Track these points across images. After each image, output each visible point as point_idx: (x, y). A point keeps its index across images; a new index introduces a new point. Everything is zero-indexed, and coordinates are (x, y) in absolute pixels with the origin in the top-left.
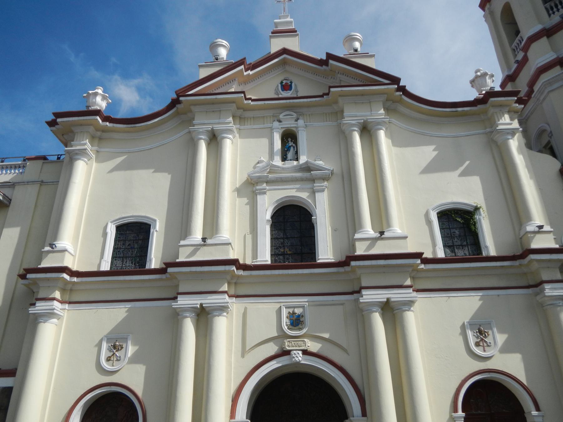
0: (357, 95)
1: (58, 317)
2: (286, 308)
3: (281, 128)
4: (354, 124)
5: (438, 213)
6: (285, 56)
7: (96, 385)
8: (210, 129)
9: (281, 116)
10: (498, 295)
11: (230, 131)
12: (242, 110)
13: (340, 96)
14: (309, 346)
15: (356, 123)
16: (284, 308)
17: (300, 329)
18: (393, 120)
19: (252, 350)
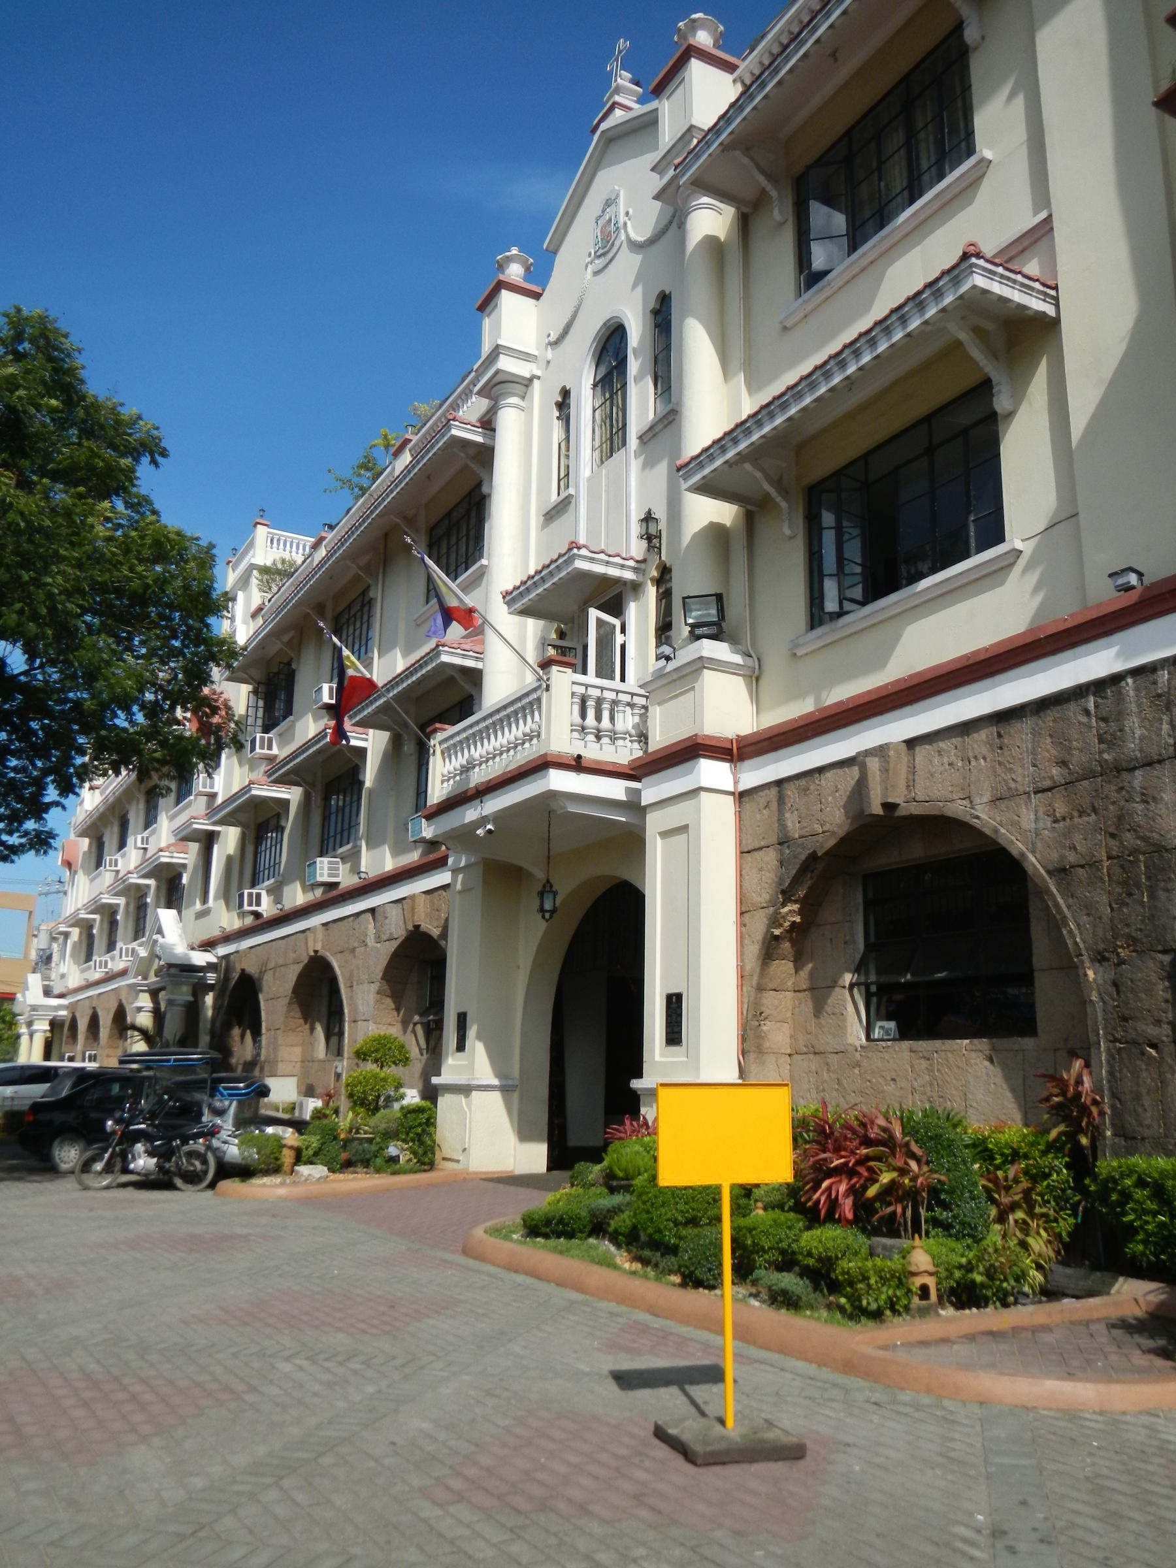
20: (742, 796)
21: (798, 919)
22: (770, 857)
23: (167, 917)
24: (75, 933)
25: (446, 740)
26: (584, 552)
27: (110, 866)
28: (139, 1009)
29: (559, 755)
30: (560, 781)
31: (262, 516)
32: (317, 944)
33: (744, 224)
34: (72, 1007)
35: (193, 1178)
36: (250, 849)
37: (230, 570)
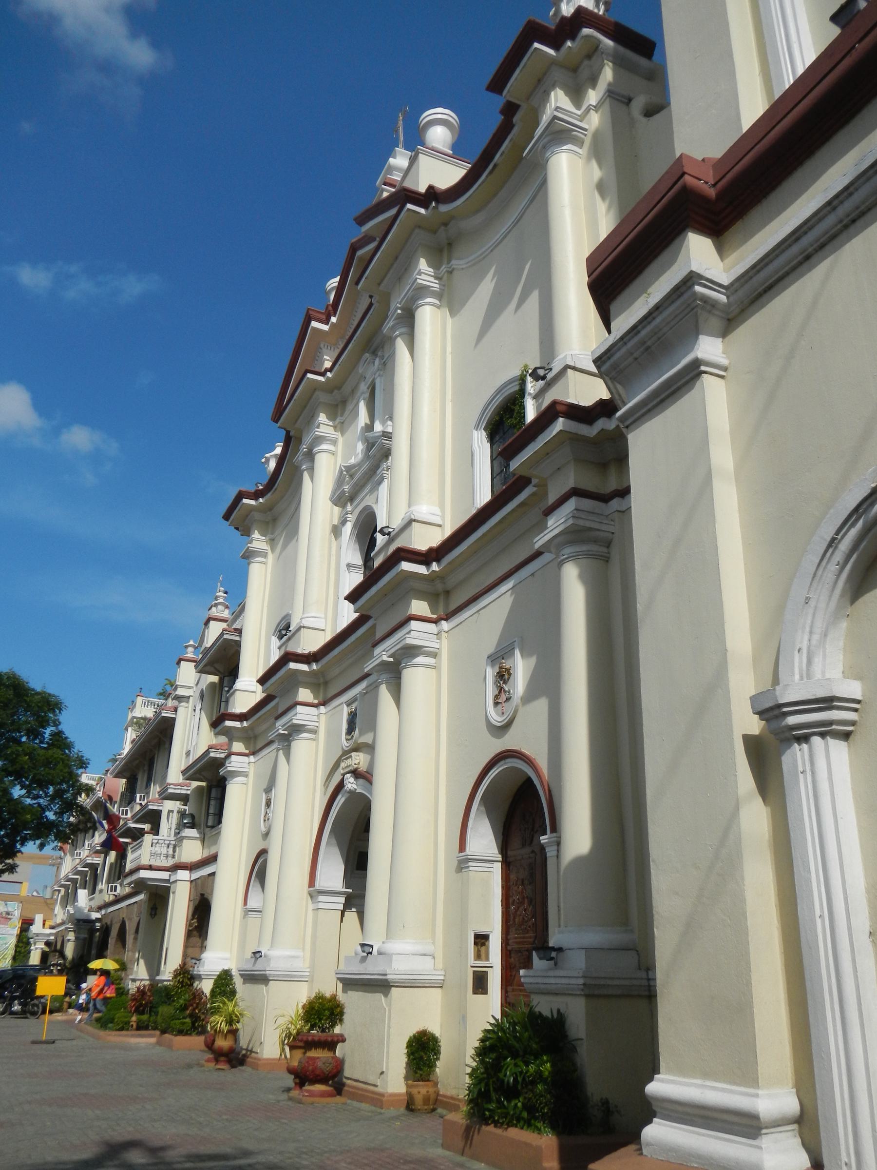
0: (392, 265)
1: (246, 775)
2: (348, 706)
3: (368, 388)
4: (393, 326)
5: (484, 429)
6: (360, 253)
7: (257, 852)
8: (305, 450)
9: (360, 371)
10: (533, 575)
11: (319, 440)
12: (336, 391)
13: (379, 284)
14: (355, 764)
15: (394, 322)
16: (345, 707)
17: (353, 736)
18: (454, 262)
19: (329, 783)
20: (191, 882)
21: (196, 924)
22: (192, 903)
23: (82, 894)
24: (63, 890)
25: (133, 847)
26: (172, 786)
27: (77, 856)
28: (69, 940)
29: (144, 865)
30: (144, 874)
31: (140, 692)
32: (123, 915)
33: (221, 680)
34: (56, 935)
35: (34, 1014)
36: (119, 861)
37: (130, 712)
